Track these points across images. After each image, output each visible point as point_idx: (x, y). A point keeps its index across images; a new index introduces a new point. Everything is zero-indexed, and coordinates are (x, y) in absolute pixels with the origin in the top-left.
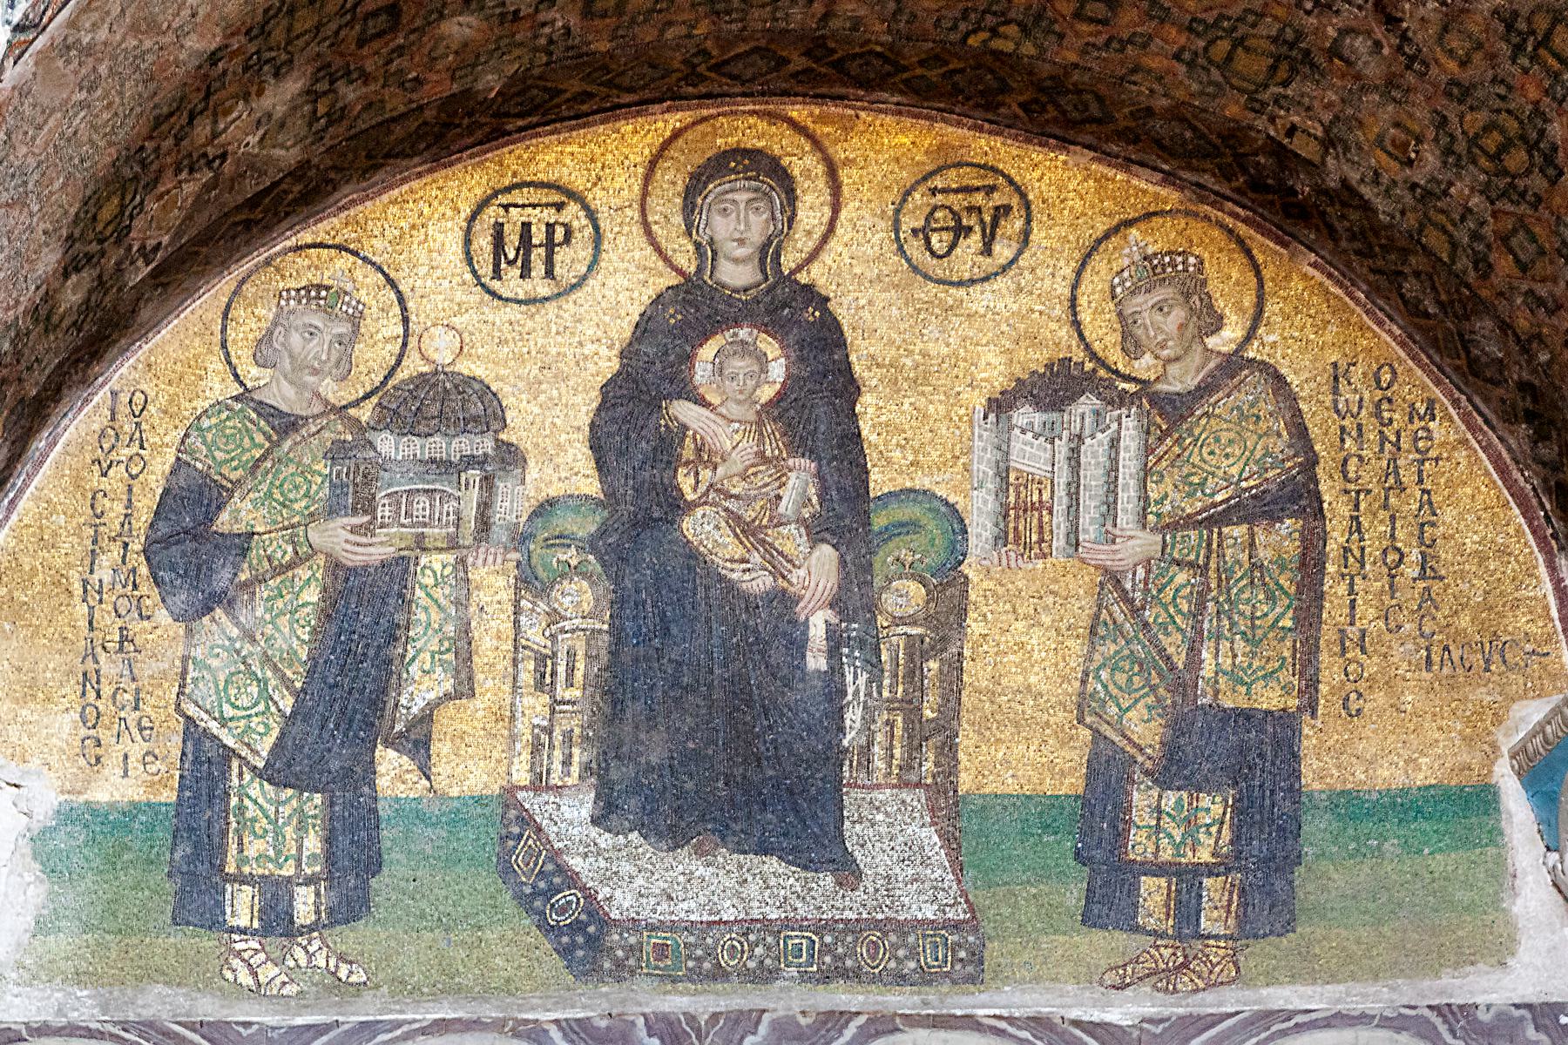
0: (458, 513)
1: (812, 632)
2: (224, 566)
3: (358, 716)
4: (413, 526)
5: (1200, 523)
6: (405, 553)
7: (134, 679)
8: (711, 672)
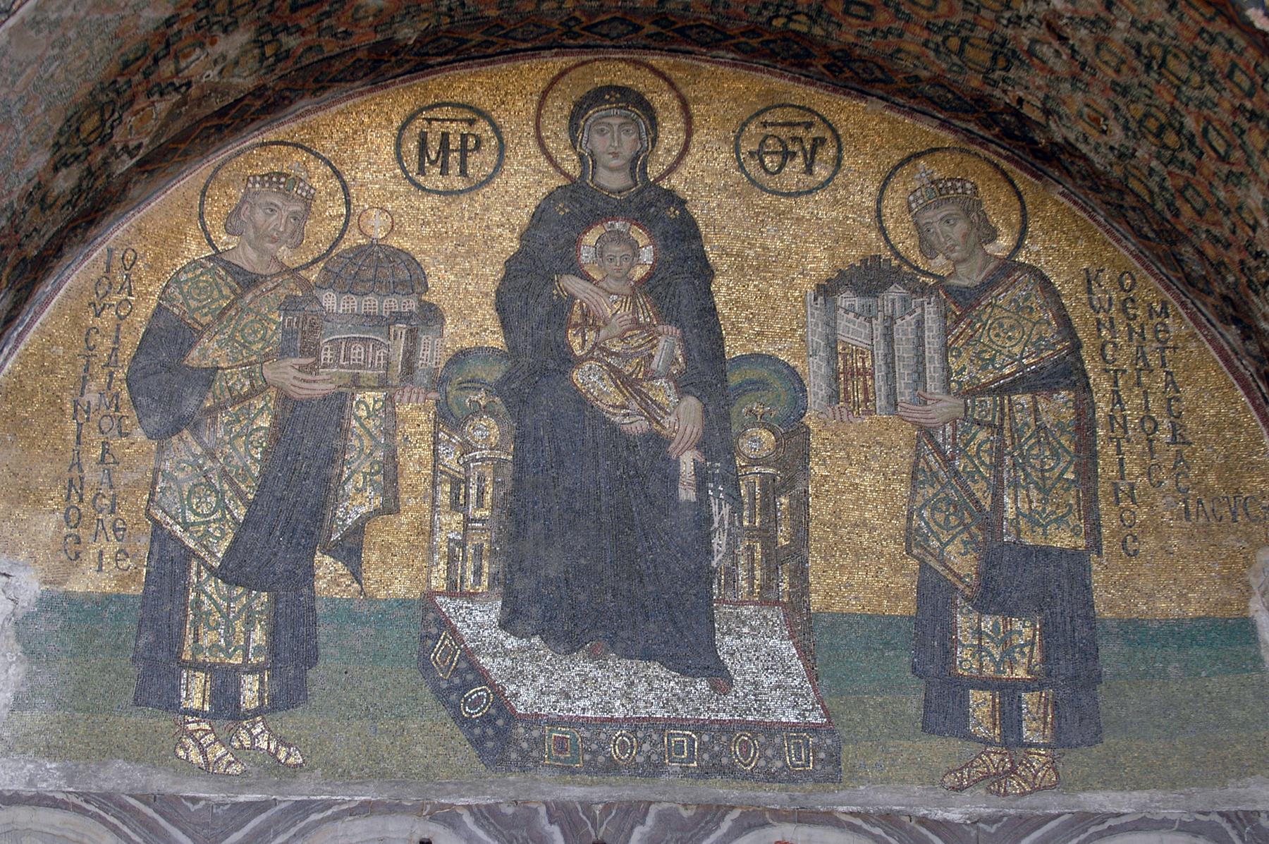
0: (387, 358)
1: (683, 468)
2: (192, 394)
3: (301, 526)
4: (350, 367)
5: (994, 390)
6: (344, 389)
7: (111, 487)
8: (599, 499)
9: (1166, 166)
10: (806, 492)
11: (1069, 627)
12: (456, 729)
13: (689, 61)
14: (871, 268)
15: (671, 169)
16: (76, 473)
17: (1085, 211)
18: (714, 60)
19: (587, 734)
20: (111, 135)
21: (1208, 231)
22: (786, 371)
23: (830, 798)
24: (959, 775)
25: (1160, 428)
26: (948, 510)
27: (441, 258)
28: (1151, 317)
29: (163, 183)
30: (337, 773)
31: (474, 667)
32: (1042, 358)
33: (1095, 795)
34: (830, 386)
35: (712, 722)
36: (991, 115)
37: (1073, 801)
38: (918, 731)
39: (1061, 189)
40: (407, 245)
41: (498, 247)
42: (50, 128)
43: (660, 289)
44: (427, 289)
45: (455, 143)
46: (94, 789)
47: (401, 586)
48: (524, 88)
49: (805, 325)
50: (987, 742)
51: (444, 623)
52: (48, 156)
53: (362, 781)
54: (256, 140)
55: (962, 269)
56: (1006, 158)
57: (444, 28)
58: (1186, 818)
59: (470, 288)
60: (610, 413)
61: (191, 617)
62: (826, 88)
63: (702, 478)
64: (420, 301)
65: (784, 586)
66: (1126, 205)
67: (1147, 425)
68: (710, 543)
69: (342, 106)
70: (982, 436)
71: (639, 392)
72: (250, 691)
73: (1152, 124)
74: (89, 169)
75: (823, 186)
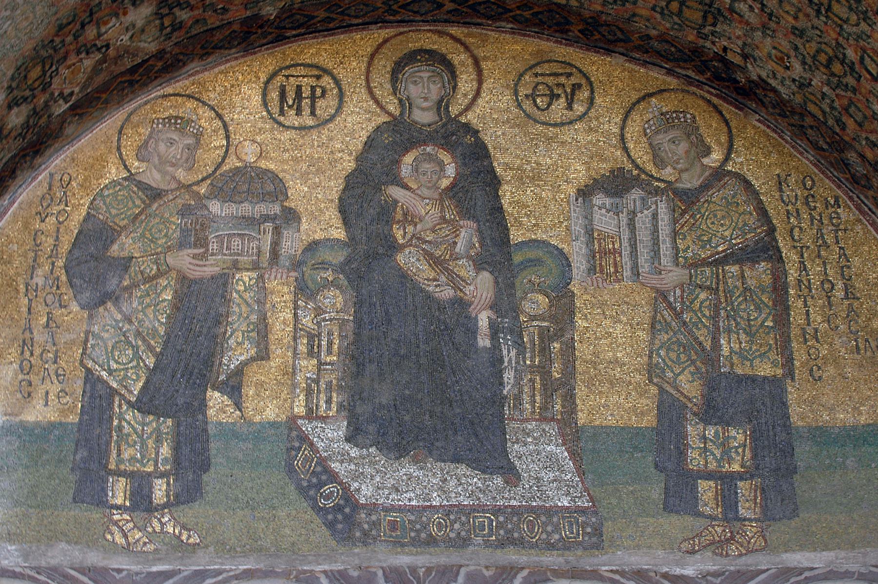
0: (259, 248)
2: (113, 276)
3: (196, 370)
5: (711, 263)
6: (227, 271)
7: (54, 344)
8: (418, 347)
9: (834, 91)
10: (573, 339)
11: (771, 433)
12: (315, 516)
13: (479, 31)
14: (617, 177)
15: (468, 108)
16: (27, 335)
17: (776, 132)
18: (498, 29)
19: (413, 518)
20: (50, 84)
21: (867, 139)
22: (555, 252)
23: (596, 560)
24: (691, 542)
25: (836, 288)
26: (679, 350)
27: (297, 175)
28: (827, 208)
29: (90, 125)
30: (225, 549)
31: (327, 471)
32: (747, 239)
33: (794, 555)
34: (588, 262)
35: (506, 507)
36: (704, 63)
37: (778, 560)
38: (660, 511)
39: (757, 117)
40: (272, 167)
41: (339, 167)
42: (4, 74)
43: (461, 195)
44: (288, 197)
45: (307, 91)
46: (43, 564)
47: (271, 412)
48: (357, 52)
49: (569, 219)
50: (712, 518)
51: (304, 438)
52: (4, 97)
53: (245, 555)
54: (159, 93)
55: (685, 176)
56: (716, 96)
57: (296, 6)
58: (863, 570)
59: (320, 196)
60: (425, 284)
61: (115, 438)
62: (581, 48)
63: (495, 330)
64: (282, 206)
65: (558, 407)
66: (806, 125)
67: (826, 286)
68: (502, 377)
69: (223, 67)
70: (703, 296)
71: (447, 269)
72: (160, 491)
73: (823, 58)
74: (34, 109)
75: (580, 118)
